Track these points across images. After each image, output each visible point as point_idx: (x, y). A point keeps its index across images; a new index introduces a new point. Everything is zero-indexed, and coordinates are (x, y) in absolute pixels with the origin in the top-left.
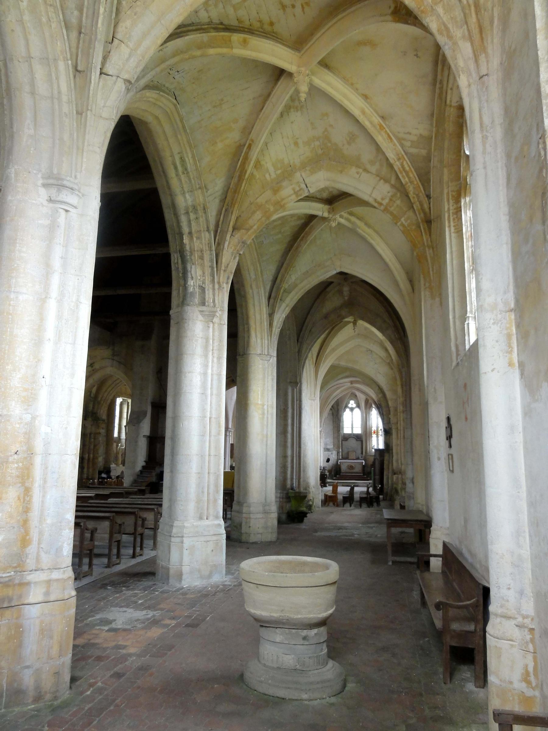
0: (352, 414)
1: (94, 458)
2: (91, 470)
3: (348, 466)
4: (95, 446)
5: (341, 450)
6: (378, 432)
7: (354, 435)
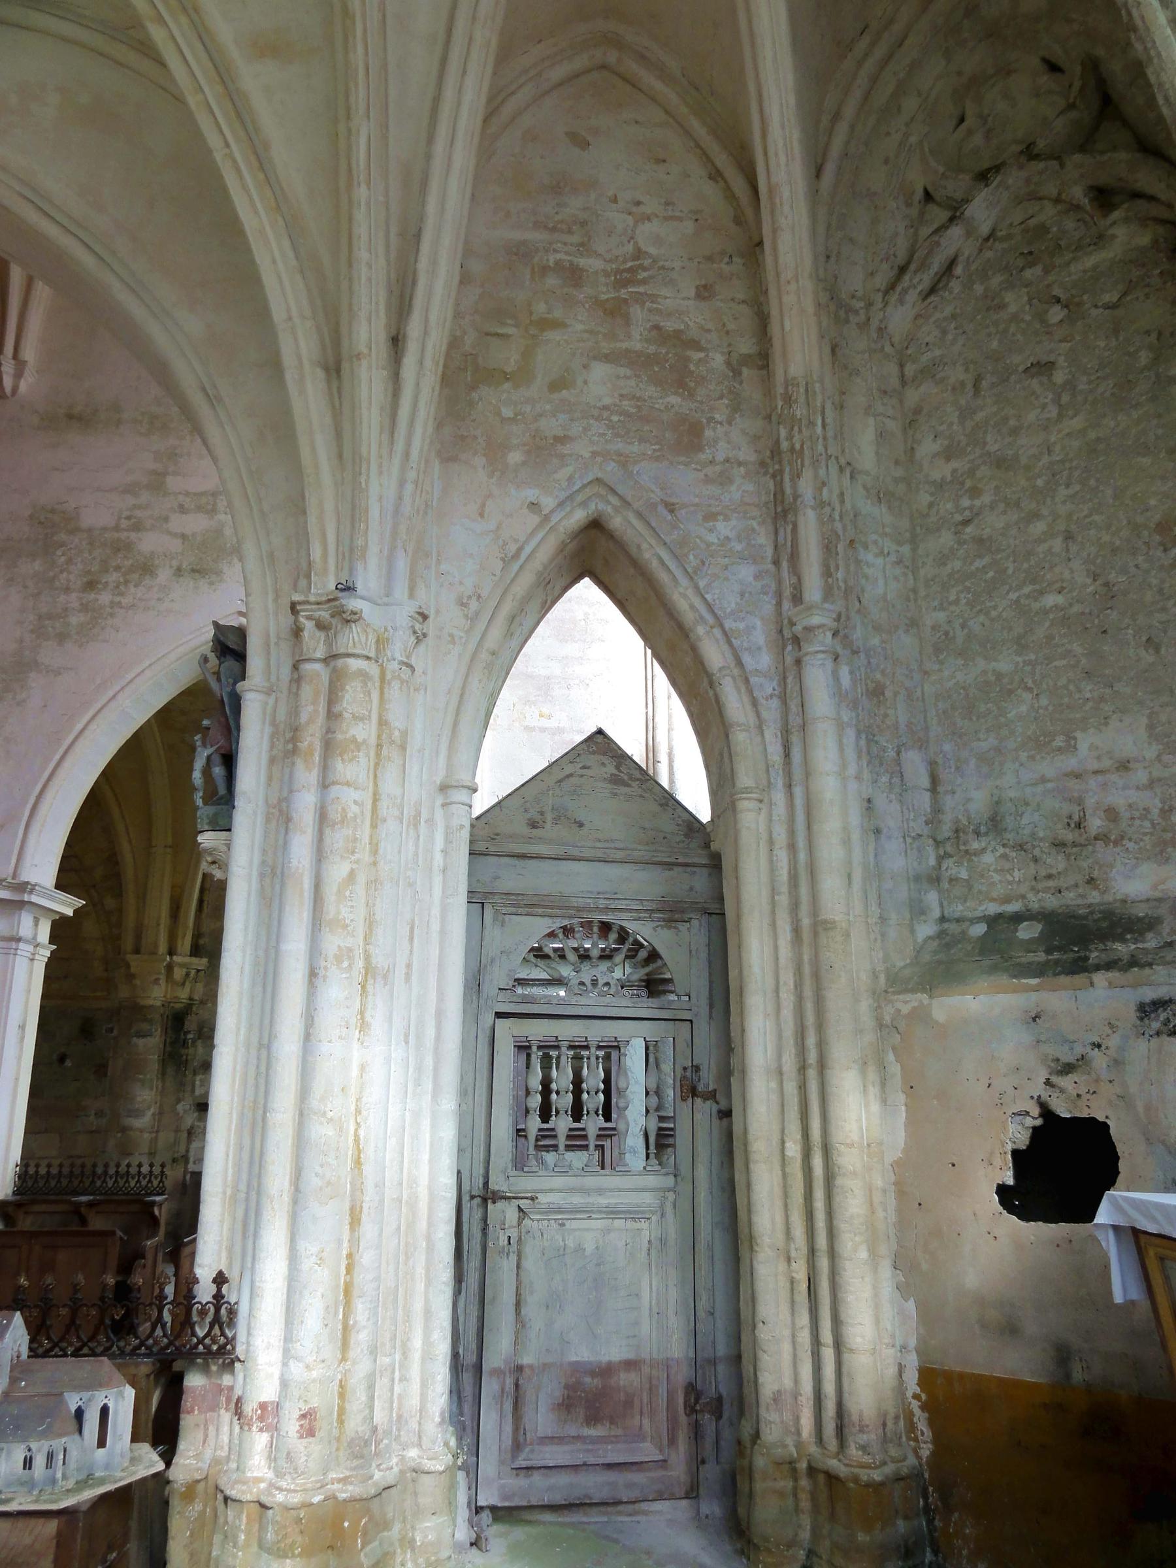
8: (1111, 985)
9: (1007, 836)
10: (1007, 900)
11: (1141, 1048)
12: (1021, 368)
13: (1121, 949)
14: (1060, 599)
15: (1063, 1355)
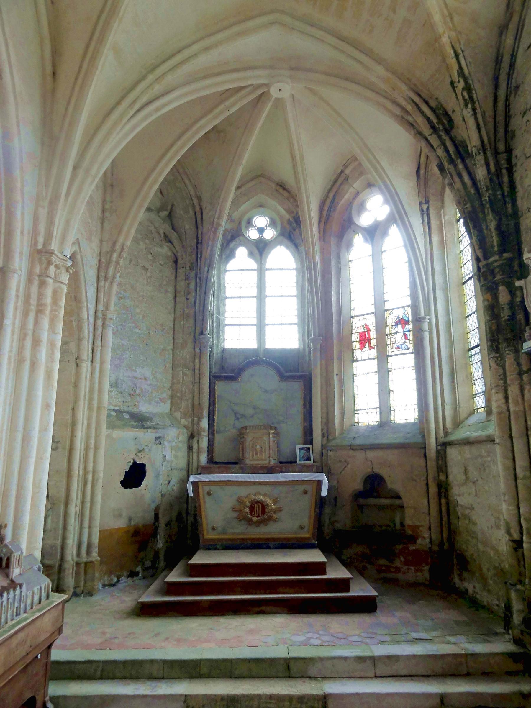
0: (261, 272)
3: (240, 501)
5: (205, 423)
6: (382, 335)
7: (268, 352)
8: (151, 433)
9: (119, 389)
10: (116, 406)
11: (155, 447)
12: (141, 265)
13: (149, 424)
14: (139, 331)
15: (130, 519)
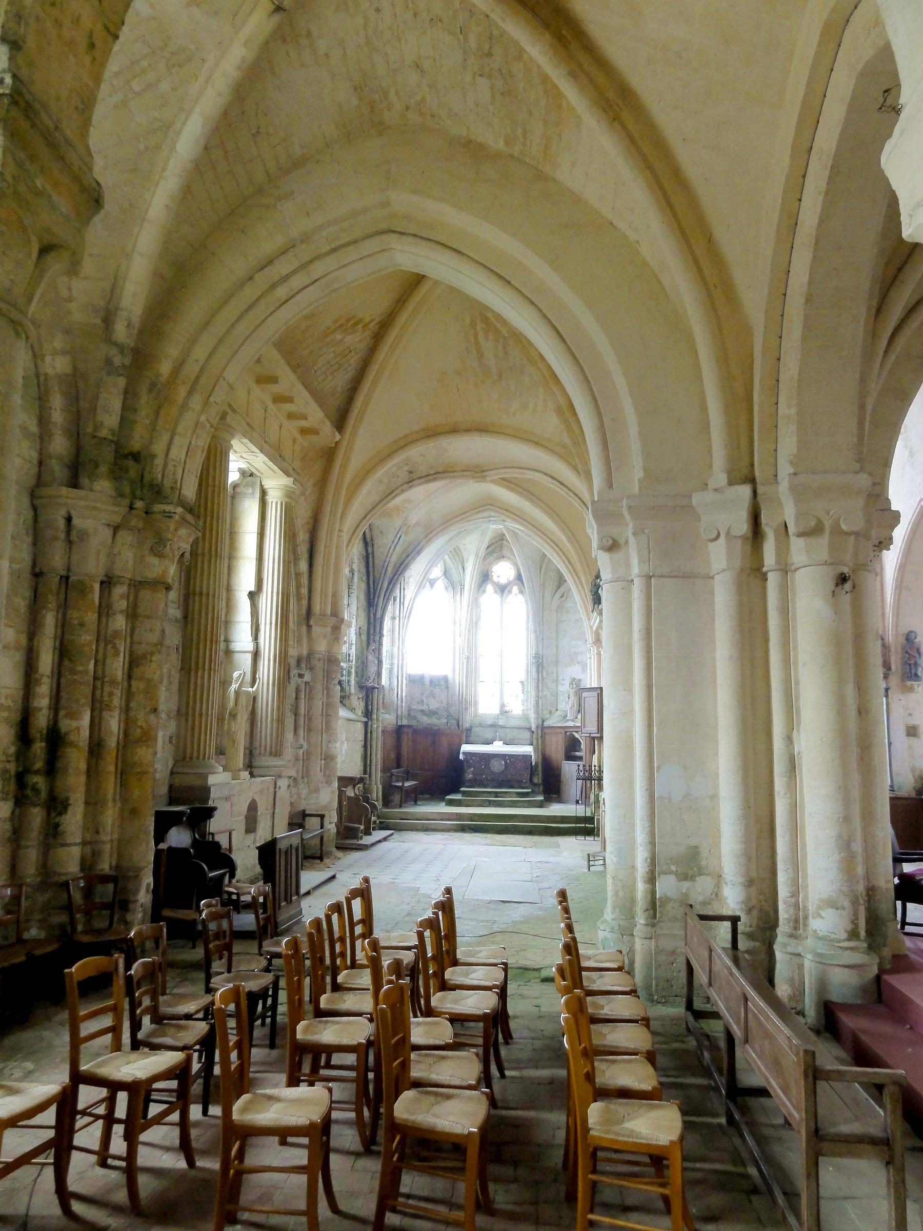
1: (127, 742)
2: (110, 816)
4: (134, 662)
